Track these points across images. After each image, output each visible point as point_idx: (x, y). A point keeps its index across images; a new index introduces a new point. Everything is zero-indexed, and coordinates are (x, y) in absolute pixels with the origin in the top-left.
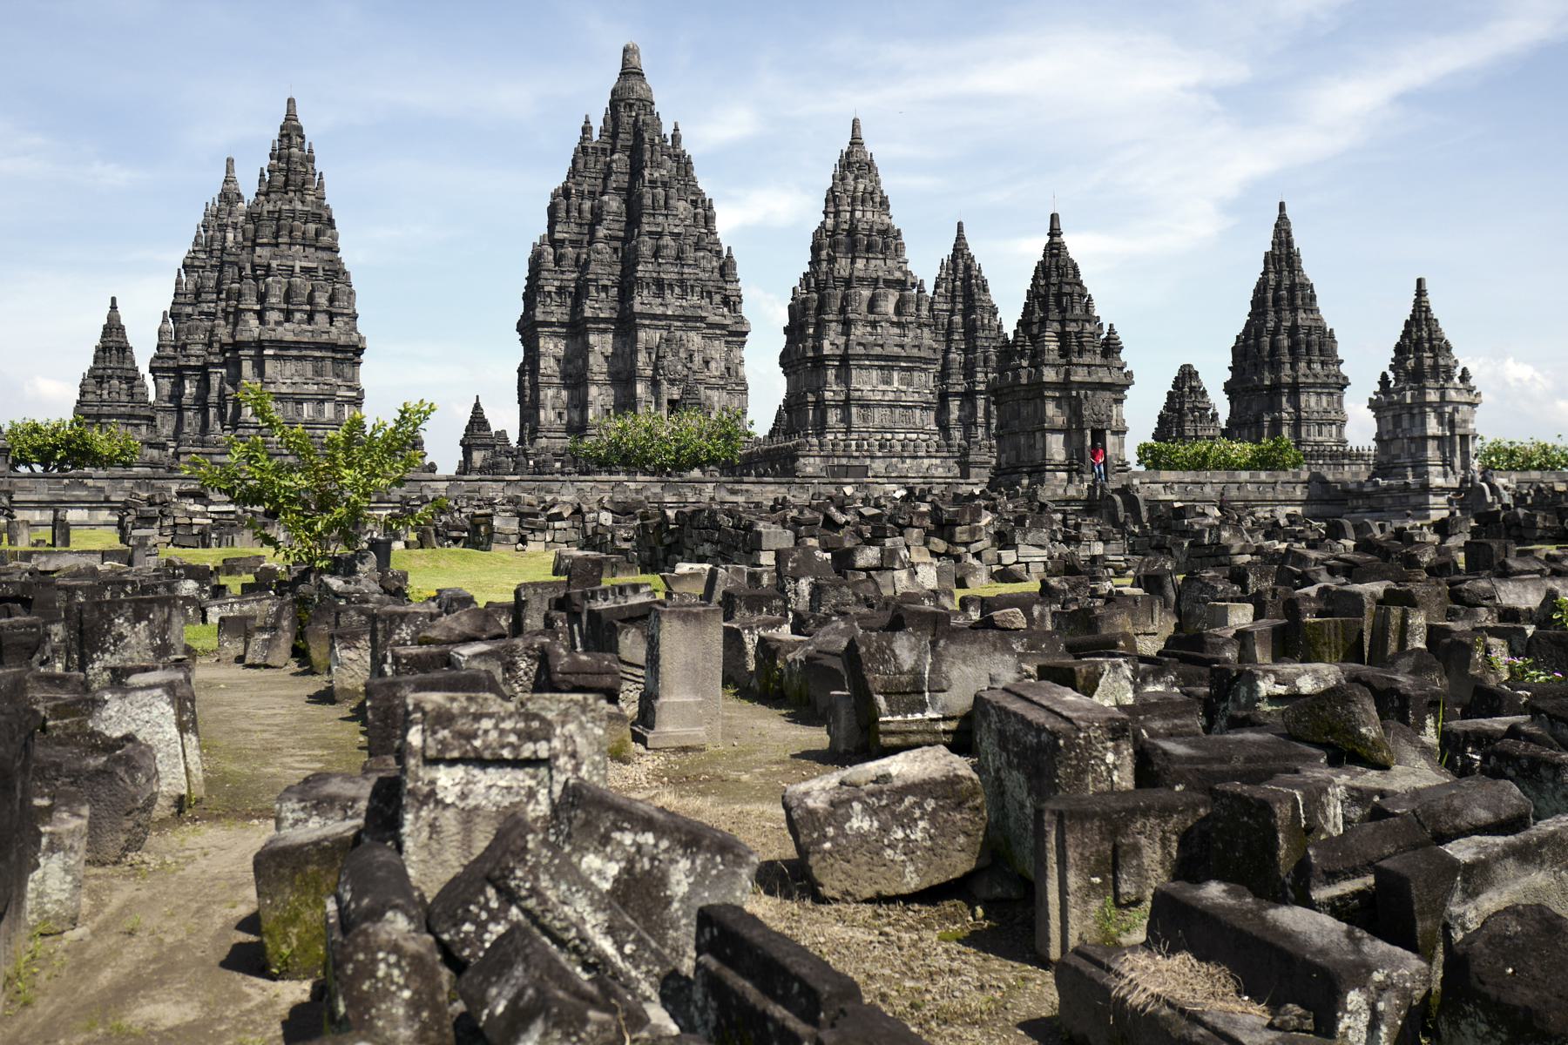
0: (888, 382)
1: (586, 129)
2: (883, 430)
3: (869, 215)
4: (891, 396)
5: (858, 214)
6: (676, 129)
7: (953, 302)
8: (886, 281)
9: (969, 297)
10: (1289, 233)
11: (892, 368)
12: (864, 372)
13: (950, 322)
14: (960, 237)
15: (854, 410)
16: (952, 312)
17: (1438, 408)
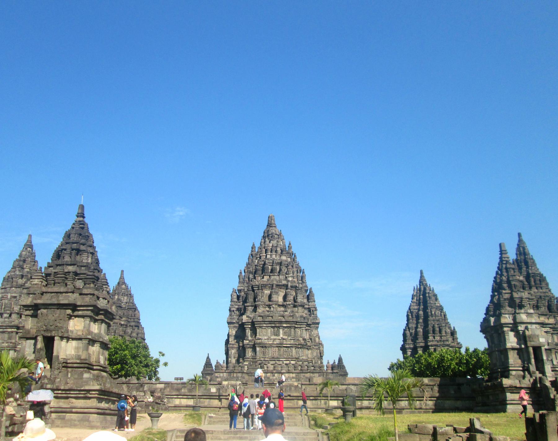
0: (278, 335)
1: (253, 247)
2: (273, 359)
3: (274, 256)
4: (277, 342)
5: (268, 256)
6: (290, 244)
7: (419, 305)
8: (277, 285)
9: (425, 303)
10: (524, 248)
11: (279, 327)
12: (264, 330)
13: (418, 313)
14: (422, 276)
15: (258, 349)
16: (419, 310)
17: (514, 327)
